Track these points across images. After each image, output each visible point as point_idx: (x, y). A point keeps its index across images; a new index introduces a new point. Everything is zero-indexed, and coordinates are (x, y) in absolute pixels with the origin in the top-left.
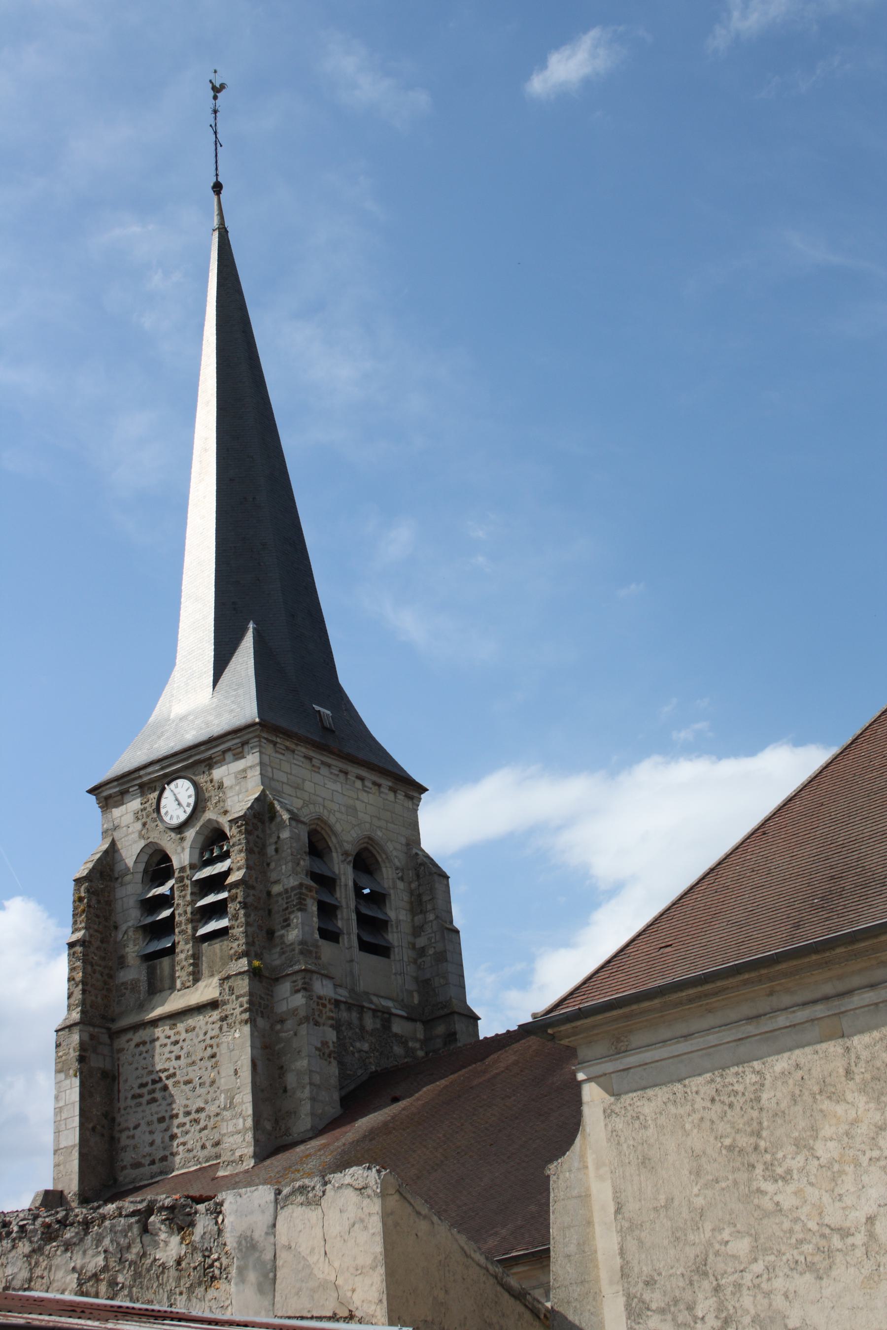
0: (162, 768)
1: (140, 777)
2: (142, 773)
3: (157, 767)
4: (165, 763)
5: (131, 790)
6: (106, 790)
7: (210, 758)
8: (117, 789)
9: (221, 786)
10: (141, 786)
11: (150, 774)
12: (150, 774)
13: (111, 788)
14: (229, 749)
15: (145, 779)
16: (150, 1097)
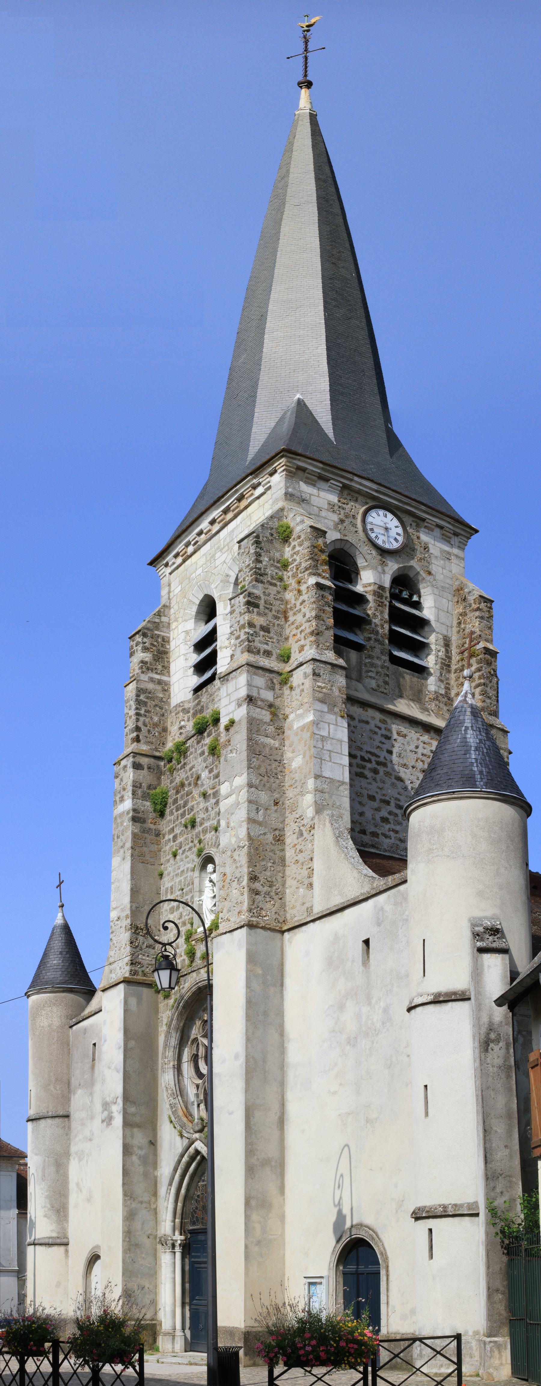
0: (376, 491)
1: (351, 480)
2: (356, 479)
3: (375, 487)
4: (382, 489)
5: (332, 481)
6: (299, 460)
7: (423, 520)
8: (319, 471)
9: (426, 548)
10: (345, 487)
11: (361, 484)
12: (361, 484)
13: (310, 464)
14: (441, 528)
15: (353, 484)
16: (359, 770)
